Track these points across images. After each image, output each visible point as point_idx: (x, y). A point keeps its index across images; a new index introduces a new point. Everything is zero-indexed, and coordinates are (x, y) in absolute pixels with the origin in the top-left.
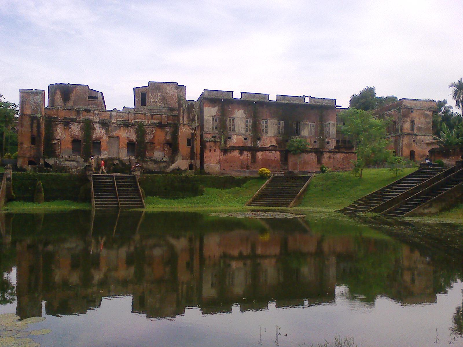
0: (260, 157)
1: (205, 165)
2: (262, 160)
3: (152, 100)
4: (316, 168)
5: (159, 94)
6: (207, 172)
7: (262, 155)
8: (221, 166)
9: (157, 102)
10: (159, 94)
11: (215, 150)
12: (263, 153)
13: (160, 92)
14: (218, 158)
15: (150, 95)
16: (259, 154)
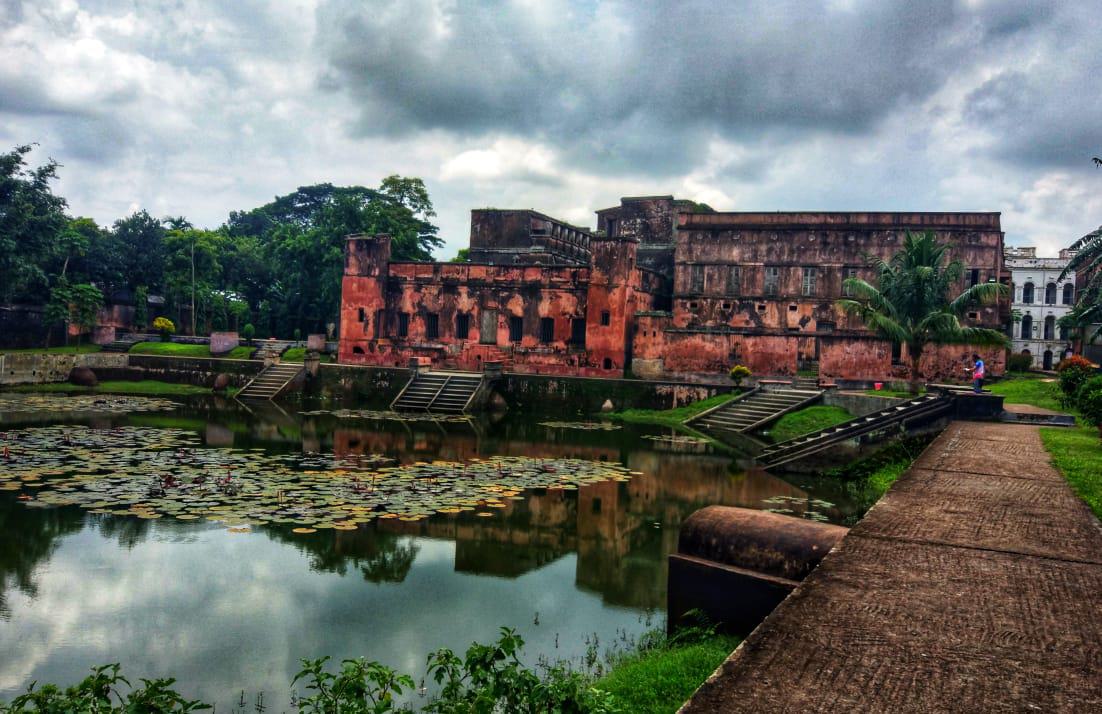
0: (750, 349)
1: (634, 360)
2: (754, 353)
3: (626, 233)
4: (889, 375)
5: (639, 220)
6: (637, 375)
7: (755, 344)
8: (664, 364)
9: (634, 236)
10: (639, 220)
11: (654, 333)
12: (758, 339)
13: (638, 216)
14: (660, 348)
15: (622, 223)
16: (750, 341)
